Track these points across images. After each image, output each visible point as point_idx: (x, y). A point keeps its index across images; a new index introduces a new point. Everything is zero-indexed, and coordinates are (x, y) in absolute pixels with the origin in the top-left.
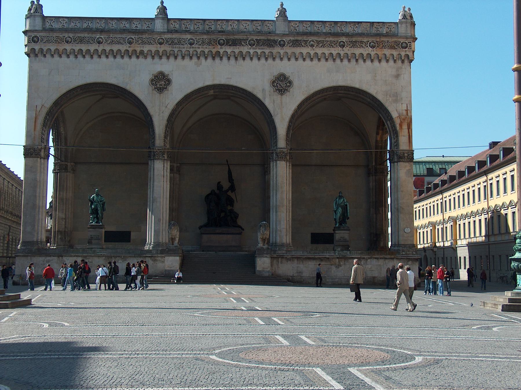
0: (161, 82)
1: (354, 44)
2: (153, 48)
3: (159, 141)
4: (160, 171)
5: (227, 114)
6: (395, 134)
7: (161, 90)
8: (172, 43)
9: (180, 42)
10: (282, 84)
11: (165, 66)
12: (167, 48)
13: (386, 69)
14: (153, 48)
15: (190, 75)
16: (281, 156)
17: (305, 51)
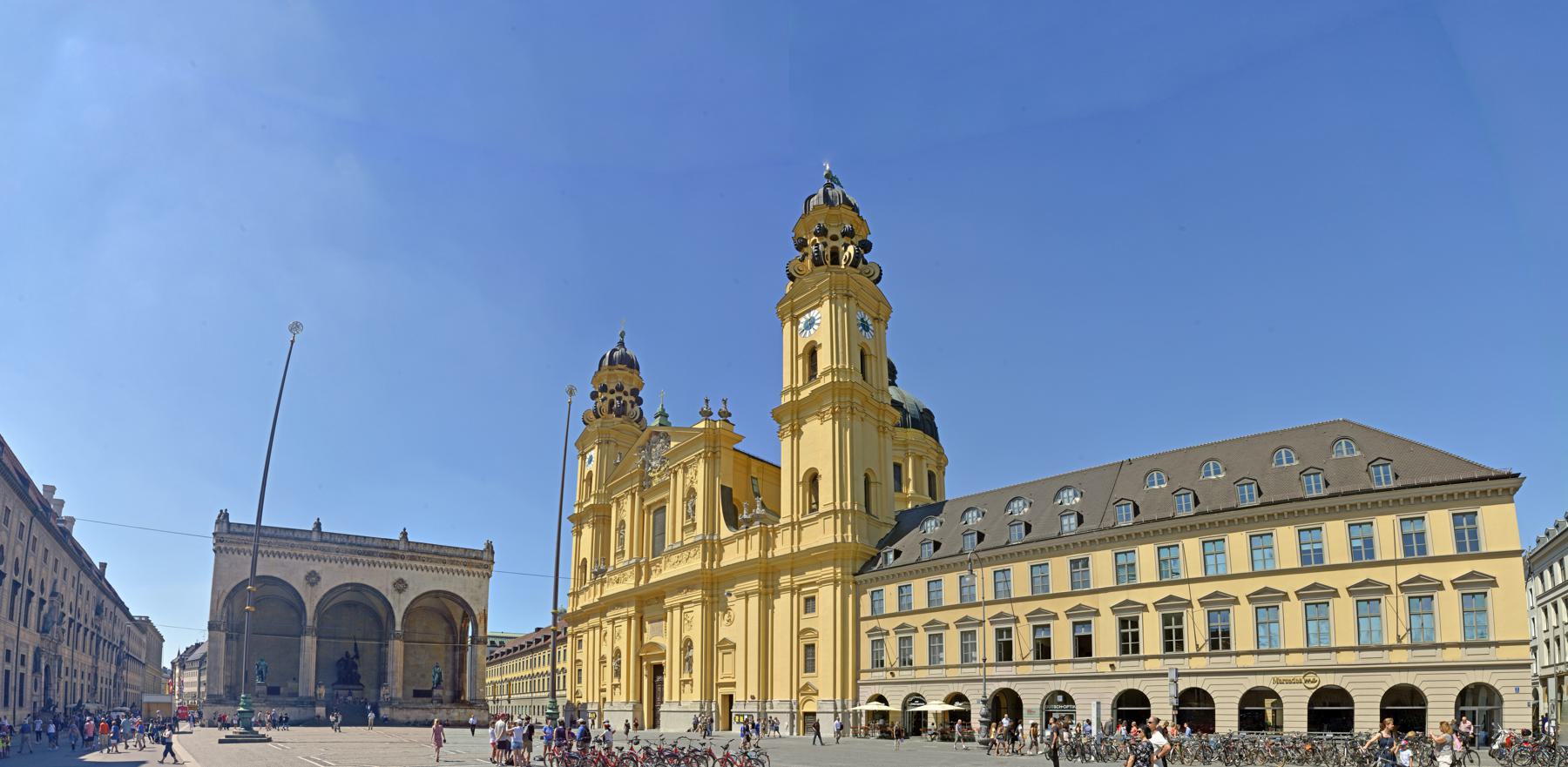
0: (313, 579)
1: (452, 563)
2: (309, 552)
3: (309, 623)
4: (309, 642)
5: (359, 607)
6: (475, 626)
7: (312, 584)
8: (323, 550)
9: (329, 550)
10: (400, 586)
11: (317, 567)
12: (319, 553)
13: (474, 580)
14: (309, 552)
15: (335, 575)
16: (397, 637)
17: (418, 564)
